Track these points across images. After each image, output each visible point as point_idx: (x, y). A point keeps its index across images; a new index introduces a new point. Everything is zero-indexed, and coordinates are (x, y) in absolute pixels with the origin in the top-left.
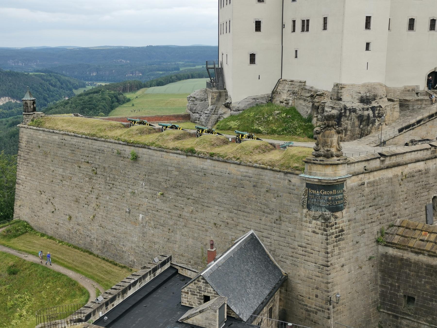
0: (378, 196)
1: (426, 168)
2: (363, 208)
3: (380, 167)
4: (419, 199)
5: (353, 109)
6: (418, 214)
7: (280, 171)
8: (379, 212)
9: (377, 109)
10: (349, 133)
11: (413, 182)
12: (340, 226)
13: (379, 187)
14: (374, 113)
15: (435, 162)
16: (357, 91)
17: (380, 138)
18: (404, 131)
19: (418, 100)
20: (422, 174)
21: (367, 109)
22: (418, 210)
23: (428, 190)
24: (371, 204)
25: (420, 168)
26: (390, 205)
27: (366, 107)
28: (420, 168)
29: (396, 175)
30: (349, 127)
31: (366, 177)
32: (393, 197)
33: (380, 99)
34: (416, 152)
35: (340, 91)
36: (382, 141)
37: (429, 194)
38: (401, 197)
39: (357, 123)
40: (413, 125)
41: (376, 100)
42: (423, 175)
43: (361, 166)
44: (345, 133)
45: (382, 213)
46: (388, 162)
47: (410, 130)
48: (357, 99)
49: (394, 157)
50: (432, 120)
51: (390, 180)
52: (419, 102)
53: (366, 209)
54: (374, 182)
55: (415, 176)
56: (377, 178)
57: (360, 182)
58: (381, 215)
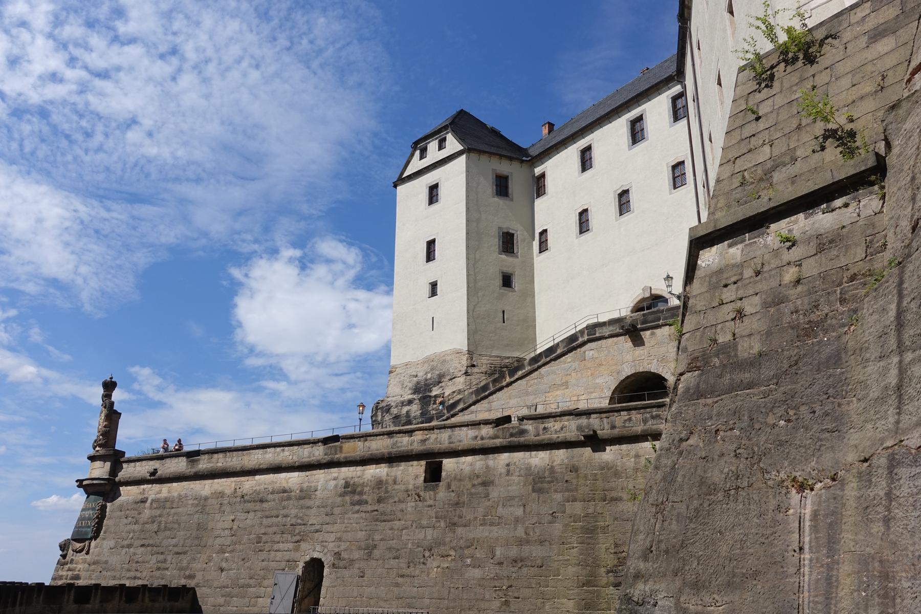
0: (166, 529)
1: (305, 485)
2: (129, 546)
4: (263, 555)
6: (251, 589)
8: (158, 562)
9: (435, 401)
11: (259, 514)
12: (76, 568)
13: (173, 511)
15: (335, 475)
20: (289, 498)
22: (252, 582)
23: (298, 538)
24: (146, 542)
26: (185, 553)
28: (285, 485)
29: (220, 493)
31: (153, 488)
32: (197, 538)
33: (451, 379)
34: (278, 449)
37: (297, 549)
38: (218, 541)
41: (440, 384)
42: (291, 502)
43: (147, 467)
45: (163, 565)
46: (204, 464)
48: (410, 389)
49: (221, 455)
51: (202, 502)
53: (132, 550)
54: (166, 500)
55: (267, 501)
56: (176, 494)
57: (140, 497)
58: (158, 569)
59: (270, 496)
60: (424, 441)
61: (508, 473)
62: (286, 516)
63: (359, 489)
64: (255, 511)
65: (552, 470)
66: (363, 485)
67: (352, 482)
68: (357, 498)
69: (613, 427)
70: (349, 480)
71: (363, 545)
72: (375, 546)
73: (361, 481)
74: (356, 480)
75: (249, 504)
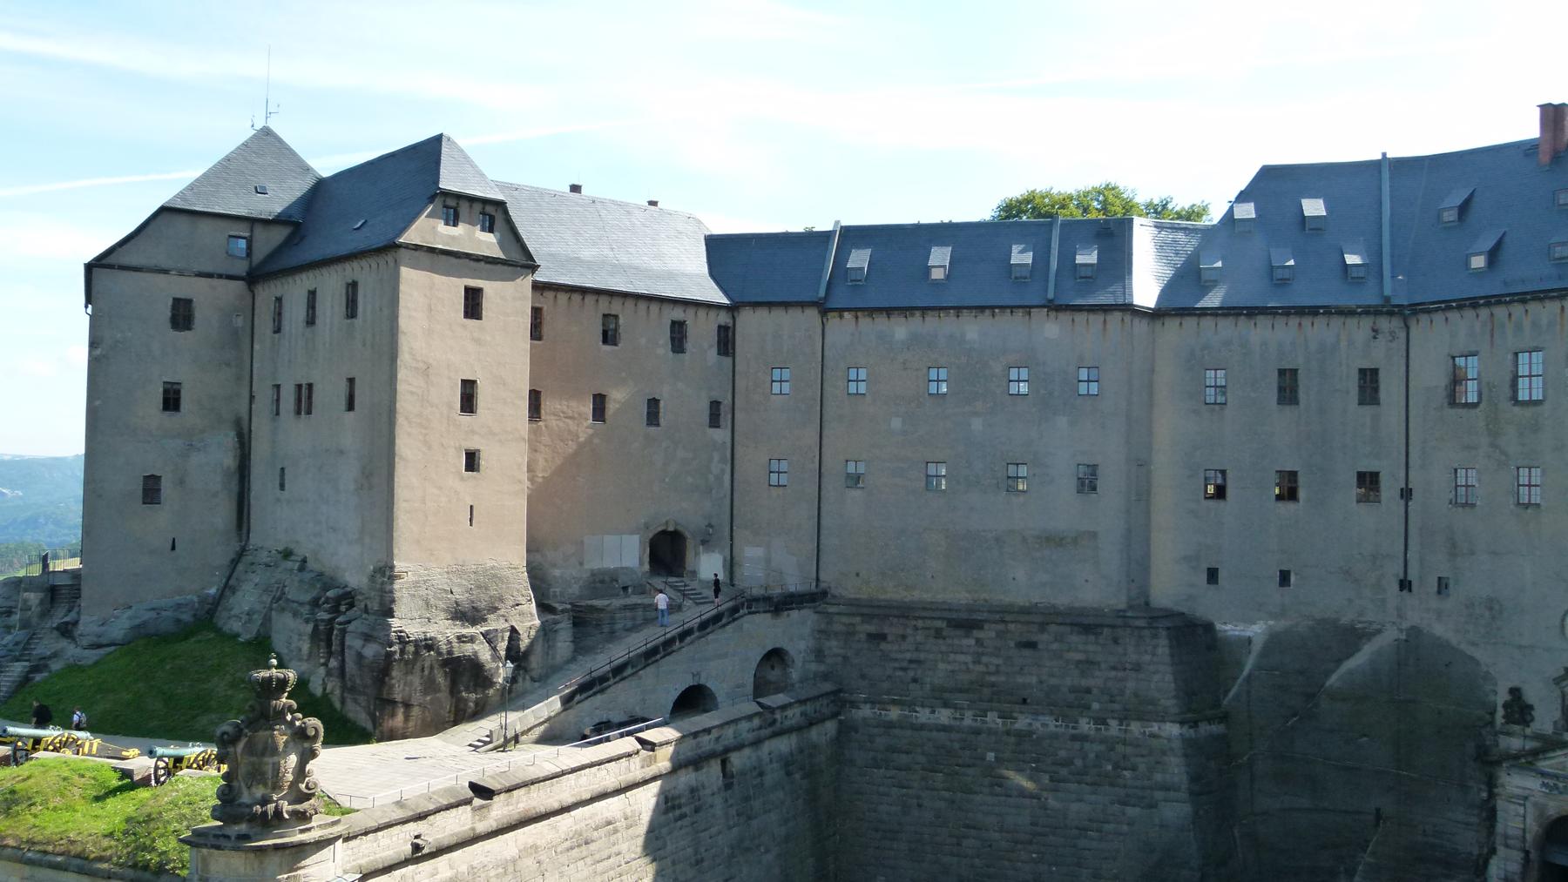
3: (473, 829)
5: (426, 639)
7: (109, 878)
10: (416, 711)
14: (494, 649)
16: (440, 587)
17: (503, 723)
18: (578, 698)
19: (625, 608)
20: (616, 831)
21: (472, 639)
25: (608, 815)
27: (469, 630)
30: (417, 698)
35: (388, 588)
36: (510, 734)
39: (441, 679)
40: (603, 679)
42: (619, 835)
43: (401, 836)
44: (404, 713)
46: (500, 811)
47: (595, 694)
49: (523, 791)
50: (653, 663)
51: (510, 866)
52: (628, 614)
55: (592, 841)
56: (464, 868)
59: (595, 833)
60: (718, 739)
61: (771, 761)
62: (619, 854)
63: (677, 802)
64: (583, 859)
65: (792, 754)
66: (679, 797)
67: (670, 796)
68: (677, 812)
69: (815, 712)
70: (667, 793)
71: (693, 861)
72: (702, 860)
73: (677, 792)
74: (673, 792)
75: (574, 851)
